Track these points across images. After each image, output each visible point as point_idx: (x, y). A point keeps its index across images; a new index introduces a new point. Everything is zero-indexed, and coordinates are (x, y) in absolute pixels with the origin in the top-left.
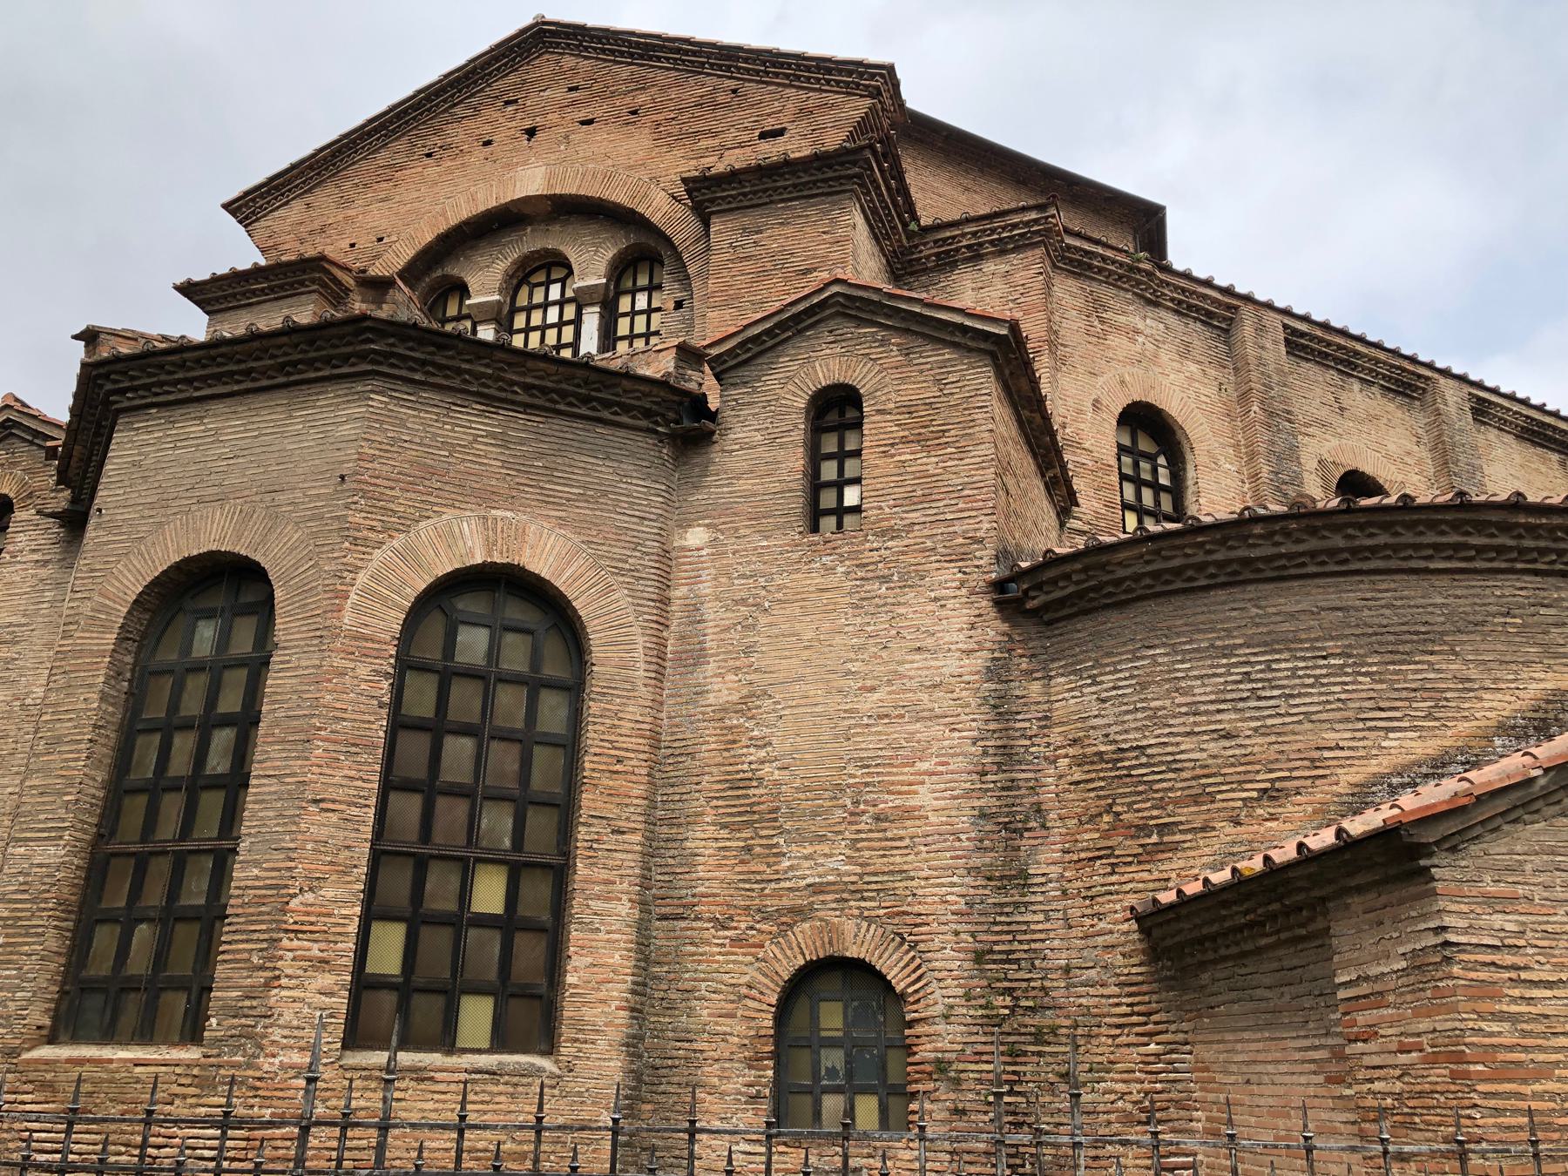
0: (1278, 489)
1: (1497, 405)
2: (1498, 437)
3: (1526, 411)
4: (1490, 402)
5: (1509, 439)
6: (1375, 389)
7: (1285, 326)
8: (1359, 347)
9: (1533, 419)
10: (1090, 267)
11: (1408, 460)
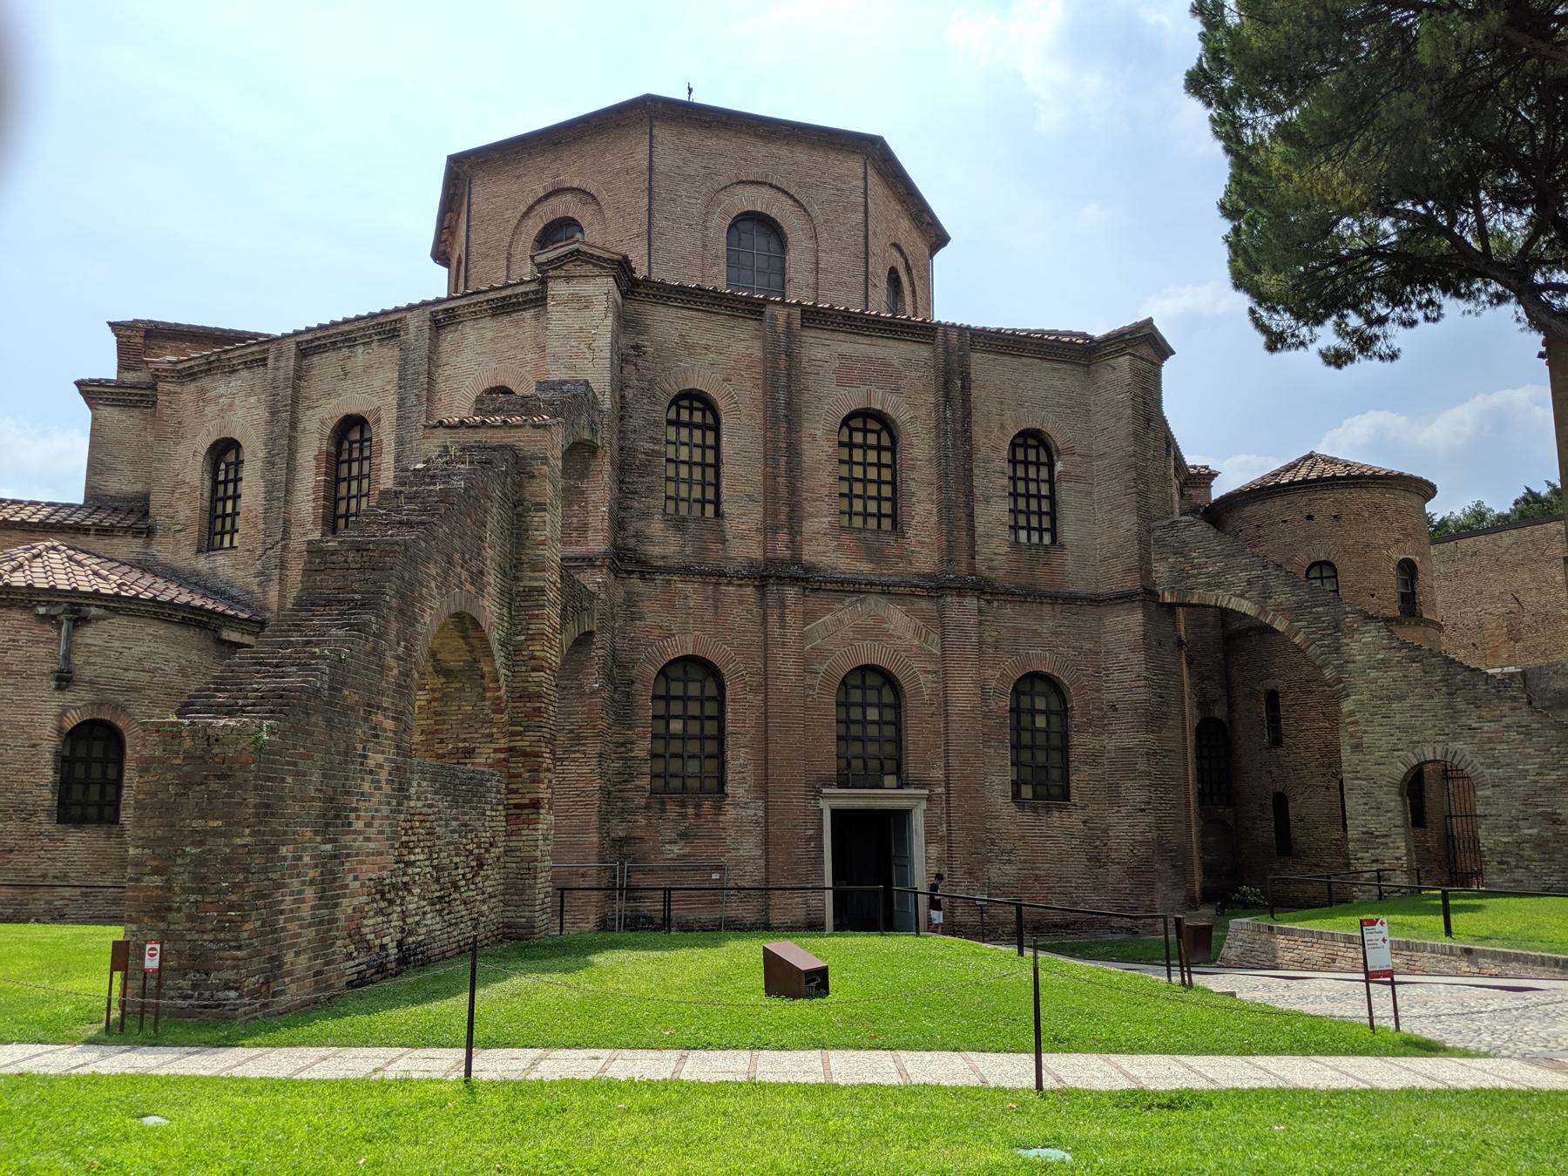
0: (269, 462)
1: (458, 307)
2: (472, 328)
3: (482, 298)
4: (453, 309)
5: (487, 323)
6: (375, 345)
7: (297, 343)
8: (347, 328)
9: (493, 300)
10: (196, 373)
11: (388, 387)
